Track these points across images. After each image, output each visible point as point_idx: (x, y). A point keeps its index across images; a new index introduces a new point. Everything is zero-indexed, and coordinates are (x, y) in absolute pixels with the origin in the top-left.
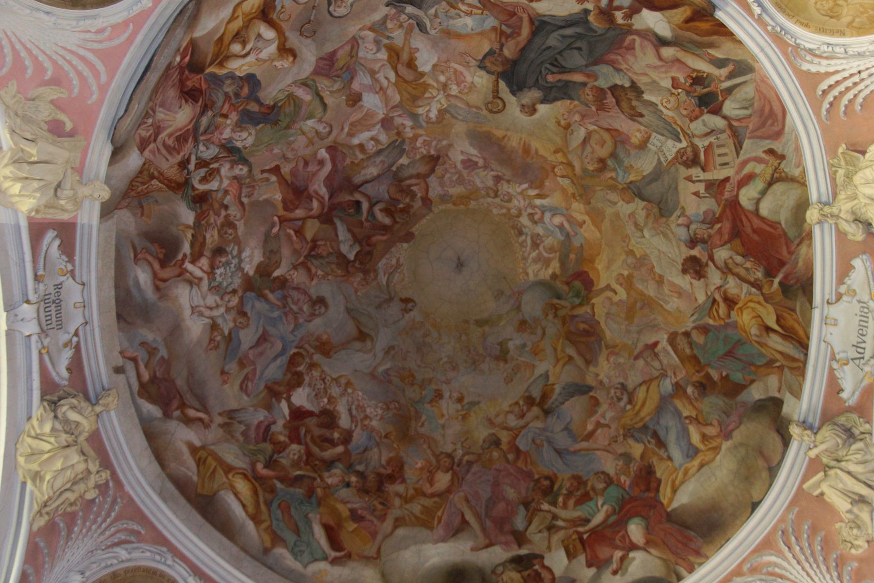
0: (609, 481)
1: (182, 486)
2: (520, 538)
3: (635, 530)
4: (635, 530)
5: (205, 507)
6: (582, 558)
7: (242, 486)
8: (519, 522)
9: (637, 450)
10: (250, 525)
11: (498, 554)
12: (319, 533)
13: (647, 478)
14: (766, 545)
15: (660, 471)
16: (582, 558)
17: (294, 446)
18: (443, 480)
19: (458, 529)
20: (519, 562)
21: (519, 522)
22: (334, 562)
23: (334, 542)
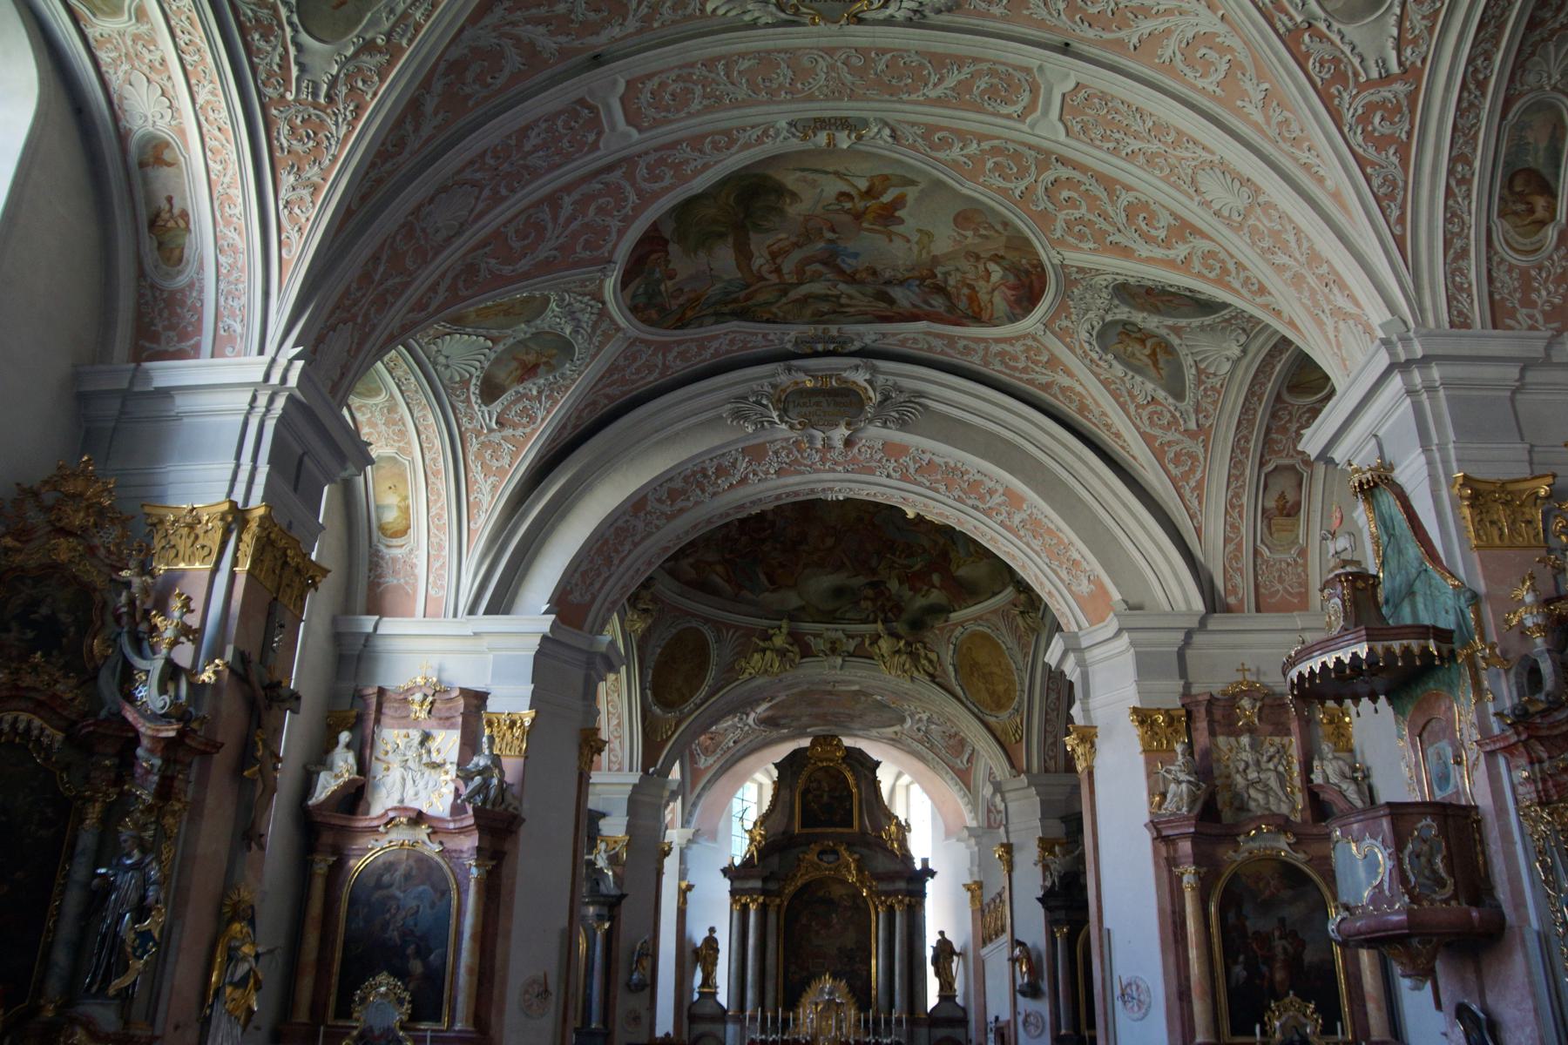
0: (925, 550)
1: (688, 583)
2: (874, 572)
3: (936, 578)
4: (936, 578)
5: (702, 586)
6: (906, 586)
7: (719, 568)
8: (874, 563)
9: (942, 541)
10: (727, 587)
11: (861, 580)
12: (763, 577)
13: (945, 555)
14: (995, 612)
15: (952, 555)
16: (906, 586)
17: (743, 538)
18: (830, 542)
19: (839, 567)
20: (873, 585)
21: (874, 563)
22: (773, 591)
23: (772, 581)
